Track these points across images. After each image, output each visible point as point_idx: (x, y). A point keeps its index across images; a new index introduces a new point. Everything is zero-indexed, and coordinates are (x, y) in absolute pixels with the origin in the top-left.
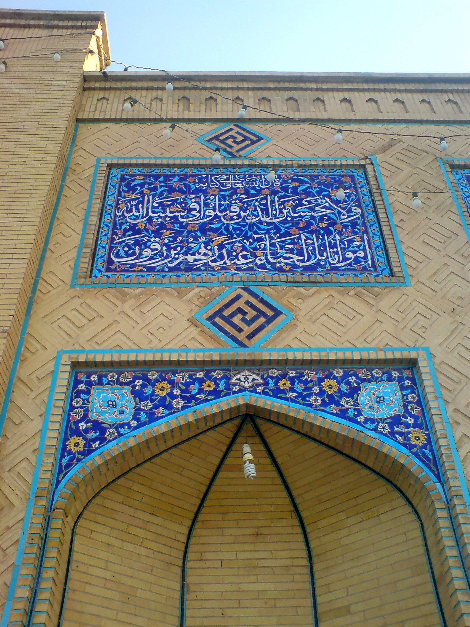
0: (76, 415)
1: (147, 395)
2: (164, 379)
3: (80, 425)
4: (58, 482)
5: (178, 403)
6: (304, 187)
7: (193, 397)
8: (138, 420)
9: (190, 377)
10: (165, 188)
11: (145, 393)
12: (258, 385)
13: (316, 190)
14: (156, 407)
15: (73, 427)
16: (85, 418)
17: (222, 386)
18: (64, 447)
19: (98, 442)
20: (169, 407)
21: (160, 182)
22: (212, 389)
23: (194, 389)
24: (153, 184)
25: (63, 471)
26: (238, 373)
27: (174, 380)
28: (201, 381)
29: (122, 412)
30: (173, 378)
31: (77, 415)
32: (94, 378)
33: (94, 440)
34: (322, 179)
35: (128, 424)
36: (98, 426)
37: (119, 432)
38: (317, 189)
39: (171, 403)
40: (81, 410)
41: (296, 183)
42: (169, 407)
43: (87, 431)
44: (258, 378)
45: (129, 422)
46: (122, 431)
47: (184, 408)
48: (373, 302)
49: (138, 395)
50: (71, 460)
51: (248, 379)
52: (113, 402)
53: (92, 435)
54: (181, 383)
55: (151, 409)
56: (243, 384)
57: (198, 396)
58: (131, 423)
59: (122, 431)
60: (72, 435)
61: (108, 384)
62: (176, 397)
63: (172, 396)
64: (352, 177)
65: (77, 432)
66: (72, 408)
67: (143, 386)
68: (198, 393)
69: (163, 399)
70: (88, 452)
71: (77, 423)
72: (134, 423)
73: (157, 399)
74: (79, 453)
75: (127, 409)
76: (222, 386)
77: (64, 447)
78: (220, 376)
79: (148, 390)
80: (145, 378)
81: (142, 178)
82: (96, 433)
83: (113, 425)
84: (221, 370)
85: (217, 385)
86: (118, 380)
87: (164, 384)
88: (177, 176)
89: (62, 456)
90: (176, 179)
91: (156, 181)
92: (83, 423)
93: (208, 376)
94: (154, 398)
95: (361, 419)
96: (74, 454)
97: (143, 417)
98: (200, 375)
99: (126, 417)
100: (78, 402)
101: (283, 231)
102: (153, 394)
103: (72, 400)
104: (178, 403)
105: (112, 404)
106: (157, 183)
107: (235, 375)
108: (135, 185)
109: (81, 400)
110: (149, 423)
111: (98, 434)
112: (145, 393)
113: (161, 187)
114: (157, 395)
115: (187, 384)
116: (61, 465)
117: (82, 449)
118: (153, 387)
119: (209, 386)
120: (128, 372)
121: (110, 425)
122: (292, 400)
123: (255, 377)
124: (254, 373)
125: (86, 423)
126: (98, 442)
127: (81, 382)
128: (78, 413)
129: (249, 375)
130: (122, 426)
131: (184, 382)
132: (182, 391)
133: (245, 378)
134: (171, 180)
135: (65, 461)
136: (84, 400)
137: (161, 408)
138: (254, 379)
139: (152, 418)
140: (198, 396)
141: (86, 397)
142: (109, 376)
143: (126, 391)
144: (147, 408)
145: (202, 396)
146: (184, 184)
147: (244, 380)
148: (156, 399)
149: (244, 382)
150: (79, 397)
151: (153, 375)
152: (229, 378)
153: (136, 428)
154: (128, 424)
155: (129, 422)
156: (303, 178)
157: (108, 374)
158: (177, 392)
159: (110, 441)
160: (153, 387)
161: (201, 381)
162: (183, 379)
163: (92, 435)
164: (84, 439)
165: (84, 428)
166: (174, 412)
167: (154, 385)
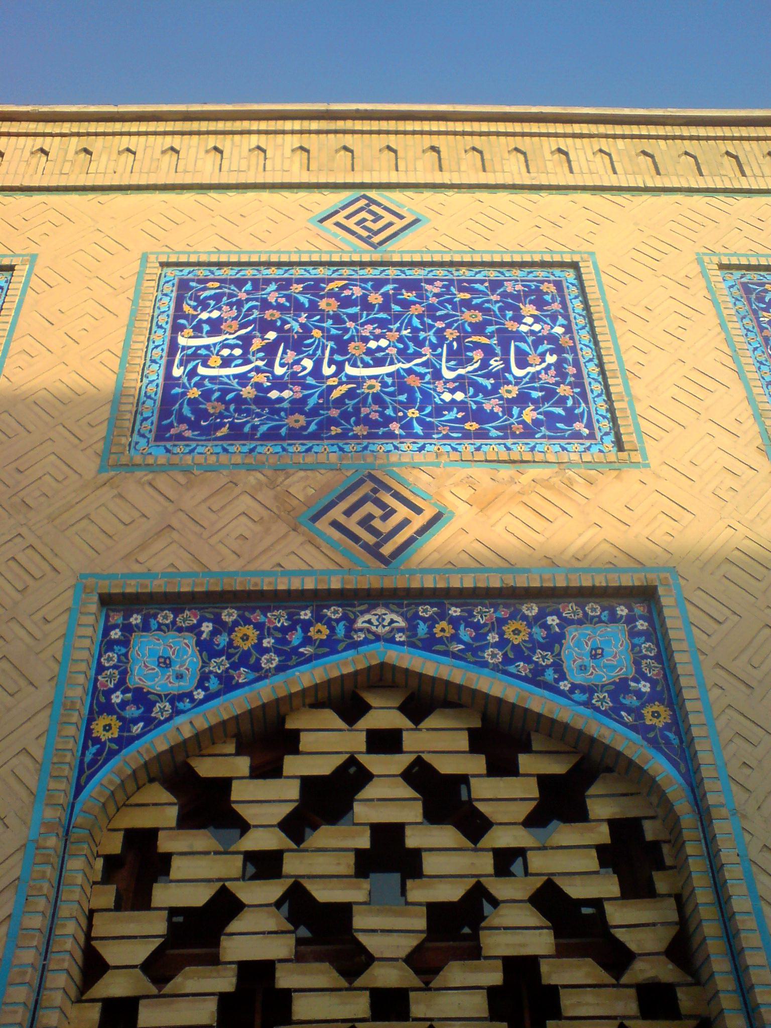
0: (107, 681)
1: (221, 646)
2: (247, 622)
3: (113, 697)
5: (270, 661)
6: (479, 301)
7: (295, 650)
8: (206, 689)
9: (290, 617)
10: (254, 303)
11: (218, 645)
12: (400, 630)
13: (498, 305)
14: (235, 666)
15: (103, 699)
16: (121, 684)
17: (341, 630)
18: (88, 732)
19: (141, 724)
20: (257, 667)
21: (248, 293)
22: (325, 637)
23: (296, 638)
24: (236, 296)
25: (85, 772)
26: (367, 611)
27: (263, 624)
29: (179, 677)
30: (261, 619)
31: (108, 681)
32: (136, 619)
33: (135, 721)
34: (509, 287)
35: (190, 695)
36: (142, 698)
37: (177, 707)
38: (501, 304)
39: (258, 660)
40: (115, 671)
41: (466, 294)
43: (123, 705)
44: (399, 619)
45: (191, 692)
46: (181, 706)
49: (207, 648)
50: (99, 753)
51: (384, 620)
52: (165, 659)
53: (132, 711)
54: (276, 628)
55: (227, 670)
56: (374, 628)
57: (301, 650)
58: (195, 693)
59: (181, 706)
60: (100, 713)
61: (159, 629)
62: (267, 651)
64: (558, 284)
65: (107, 708)
66: (101, 669)
67: (214, 633)
68: (302, 645)
69: (246, 655)
70: (124, 741)
71: (108, 693)
72: (200, 695)
73: (237, 653)
74: (112, 740)
75: (188, 669)
76: (341, 630)
77: (88, 732)
78: (338, 616)
79: (222, 640)
80: (217, 621)
81: (217, 284)
82: (138, 708)
83: (166, 696)
84: (339, 606)
85: (332, 629)
86: (174, 622)
88: (274, 283)
89: (85, 748)
90: (273, 287)
91: (240, 290)
92: (118, 693)
94: (232, 651)
96: (103, 744)
97: (214, 684)
98: (306, 614)
99: (187, 685)
100: (109, 659)
102: (230, 644)
103: (100, 656)
104: (270, 661)
105: (165, 663)
106: (243, 296)
107: (363, 613)
108: (207, 298)
109: (116, 655)
110: (225, 693)
111: (142, 709)
112: (218, 645)
113: (248, 300)
114: (238, 647)
115: (284, 630)
116: (82, 762)
117: (116, 735)
118: (230, 634)
119: (320, 632)
120: (189, 610)
121: (159, 696)
122: (454, 656)
123: (395, 617)
124: (392, 611)
125: (123, 693)
126: (141, 724)
127: (115, 627)
128: (111, 677)
129: (385, 614)
130: (181, 697)
131: (279, 625)
132: (277, 640)
133: (377, 620)
134: (264, 289)
135: (89, 757)
136: (119, 656)
137: (242, 669)
138: (392, 621)
139: (228, 685)
140: (301, 650)
141: (123, 650)
142: (159, 616)
143: (186, 641)
144: (219, 669)
145: (307, 650)
146: (285, 296)
147: (378, 623)
148: (235, 654)
149: (377, 627)
150: (113, 650)
151: (229, 615)
152: (354, 621)
154: (190, 695)
155: (191, 692)
156: (477, 286)
157: (158, 614)
158: (267, 642)
159: (161, 723)
160: (230, 634)
162: (279, 621)
163: (132, 711)
164: (120, 718)
165: (119, 701)
166: (266, 677)
167: (231, 631)
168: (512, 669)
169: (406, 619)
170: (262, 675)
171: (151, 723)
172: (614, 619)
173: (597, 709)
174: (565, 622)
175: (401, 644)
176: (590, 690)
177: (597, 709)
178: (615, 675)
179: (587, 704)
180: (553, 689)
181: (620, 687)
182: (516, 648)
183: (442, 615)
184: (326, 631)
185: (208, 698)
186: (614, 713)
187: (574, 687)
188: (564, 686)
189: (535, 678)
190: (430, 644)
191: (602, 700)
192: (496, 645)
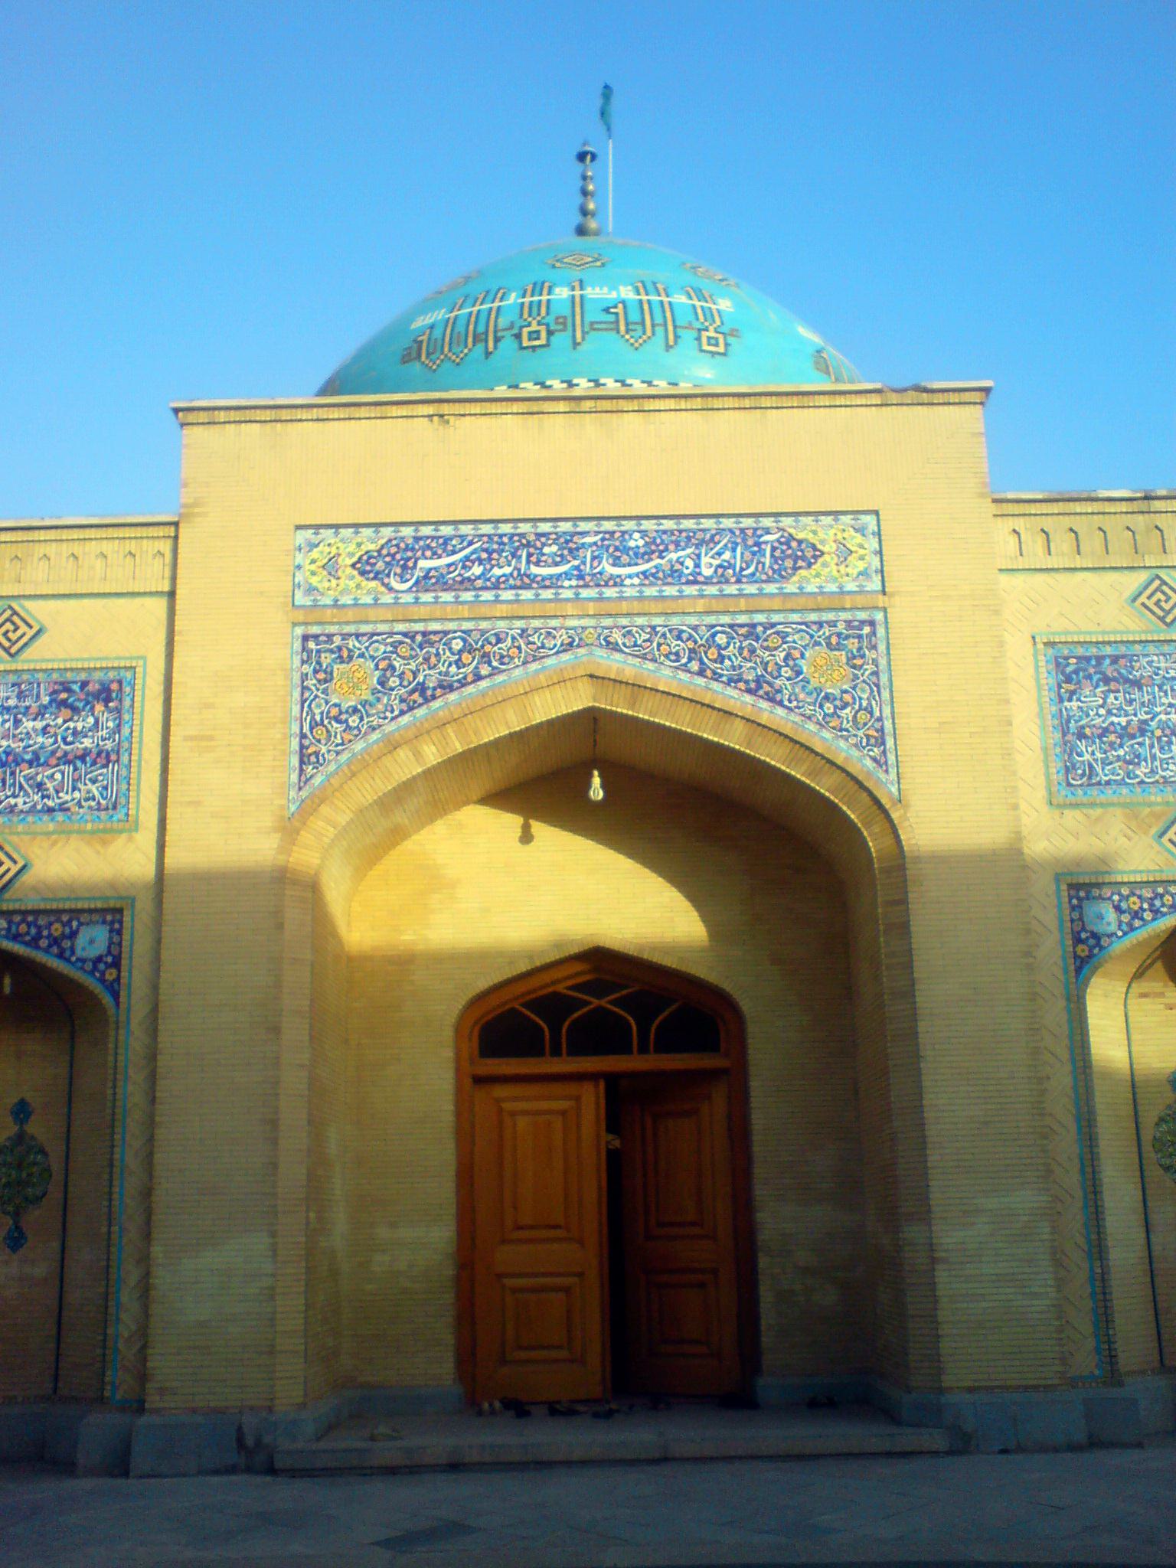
48: (102, 851)
101: (42, 760)
168: (51, 949)
172: (104, 922)
174: (81, 924)
176: (83, 960)
179: (82, 968)
180: (68, 960)
181: (99, 959)
183: (23, 921)
186: (92, 973)
187: (78, 960)
188: (74, 959)
189: (61, 956)
190: (16, 938)
191: (89, 966)
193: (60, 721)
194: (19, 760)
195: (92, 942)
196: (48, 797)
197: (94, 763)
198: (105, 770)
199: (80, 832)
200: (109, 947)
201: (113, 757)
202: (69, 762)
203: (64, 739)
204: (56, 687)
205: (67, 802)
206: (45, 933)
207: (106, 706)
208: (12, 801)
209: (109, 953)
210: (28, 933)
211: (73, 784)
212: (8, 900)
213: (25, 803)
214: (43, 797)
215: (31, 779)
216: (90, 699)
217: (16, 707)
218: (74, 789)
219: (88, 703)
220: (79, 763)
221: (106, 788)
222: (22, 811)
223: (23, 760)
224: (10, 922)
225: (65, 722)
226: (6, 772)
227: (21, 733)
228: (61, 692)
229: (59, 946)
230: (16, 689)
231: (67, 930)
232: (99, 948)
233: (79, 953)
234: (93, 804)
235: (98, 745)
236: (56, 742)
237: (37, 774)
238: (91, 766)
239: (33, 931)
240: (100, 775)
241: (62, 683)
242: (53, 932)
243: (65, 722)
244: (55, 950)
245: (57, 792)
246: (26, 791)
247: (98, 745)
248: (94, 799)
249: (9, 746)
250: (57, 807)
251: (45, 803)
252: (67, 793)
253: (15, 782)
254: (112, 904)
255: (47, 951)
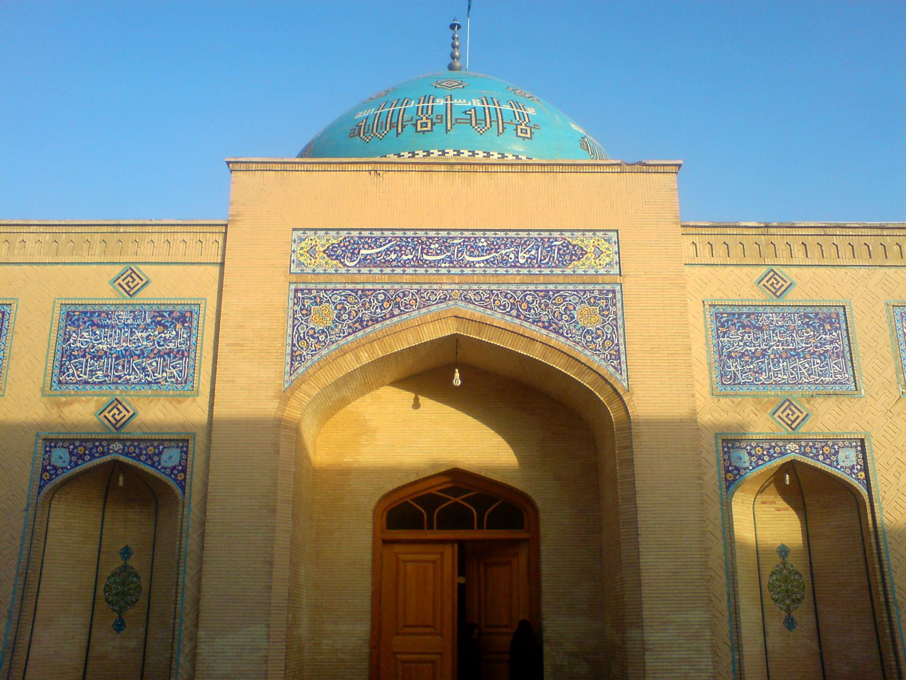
4: (39, 493)
18: (41, 477)
20: (83, 460)
28: (97, 447)
29: (64, 462)
33: (53, 475)
35: (66, 468)
42: (83, 460)
43: (50, 470)
47: (90, 460)
48: (177, 406)
50: (44, 483)
53: (52, 472)
63: (85, 454)
65: (46, 471)
69: (81, 455)
70: (50, 480)
72: (69, 467)
74: (48, 480)
87: (82, 448)
89: (41, 481)
93: (101, 445)
95: (160, 467)
96: (45, 481)
99: (66, 464)
101: (146, 355)
104: (87, 458)
115: (91, 449)
132: (89, 452)
135: (42, 484)
139: (77, 465)
153: (69, 469)
154: (66, 468)
161: (97, 447)
164: (49, 473)
168: (147, 462)
169: (123, 446)
170: (85, 461)
171: (57, 475)
172: (178, 447)
173: (166, 474)
175: (120, 453)
176: (165, 468)
177: (166, 474)
178: (174, 465)
179: (164, 473)
180: (157, 468)
181: (174, 468)
182: (150, 456)
183: (132, 445)
184: (102, 449)
185: (72, 468)
186: (170, 475)
187: (163, 468)
189: (152, 465)
190: (127, 454)
192: (145, 455)
193: (156, 333)
194: (133, 354)
195: (170, 458)
196: (148, 375)
197: (175, 357)
198: (181, 361)
199: (165, 396)
200: (180, 461)
201: (186, 354)
202: (161, 356)
203: (159, 343)
204: (155, 314)
205: (158, 379)
206: (144, 452)
207: (183, 326)
208: (128, 377)
209: (180, 464)
210: (134, 452)
211: (163, 369)
212: (123, 433)
213: (135, 378)
214: (145, 376)
215: (139, 365)
216: (174, 321)
217: (132, 324)
218: (163, 371)
219: (173, 323)
220: (166, 357)
221: (181, 371)
222: (133, 383)
223: (135, 354)
224: (124, 446)
225: (159, 333)
226: (124, 361)
227: (134, 339)
228: (157, 316)
229: (152, 459)
230: (132, 314)
231: (157, 451)
232: (175, 461)
233: (163, 464)
234: (174, 380)
235: (178, 347)
236: (154, 344)
237: (143, 362)
238: (173, 359)
239: (137, 451)
240: (178, 364)
241: (158, 312)
242: (148, 451)
243: (159, 333)
244: (149, 462)
245: (154, 373)
246: (136, 372)
247: (178, 347)
248: (174, 377)
249: (127, 346)
250: (153, 381)
251: (147, 379)
252: (159, 374)
253: (130, 366)
254: (183, 437)
255: (144, 462)
